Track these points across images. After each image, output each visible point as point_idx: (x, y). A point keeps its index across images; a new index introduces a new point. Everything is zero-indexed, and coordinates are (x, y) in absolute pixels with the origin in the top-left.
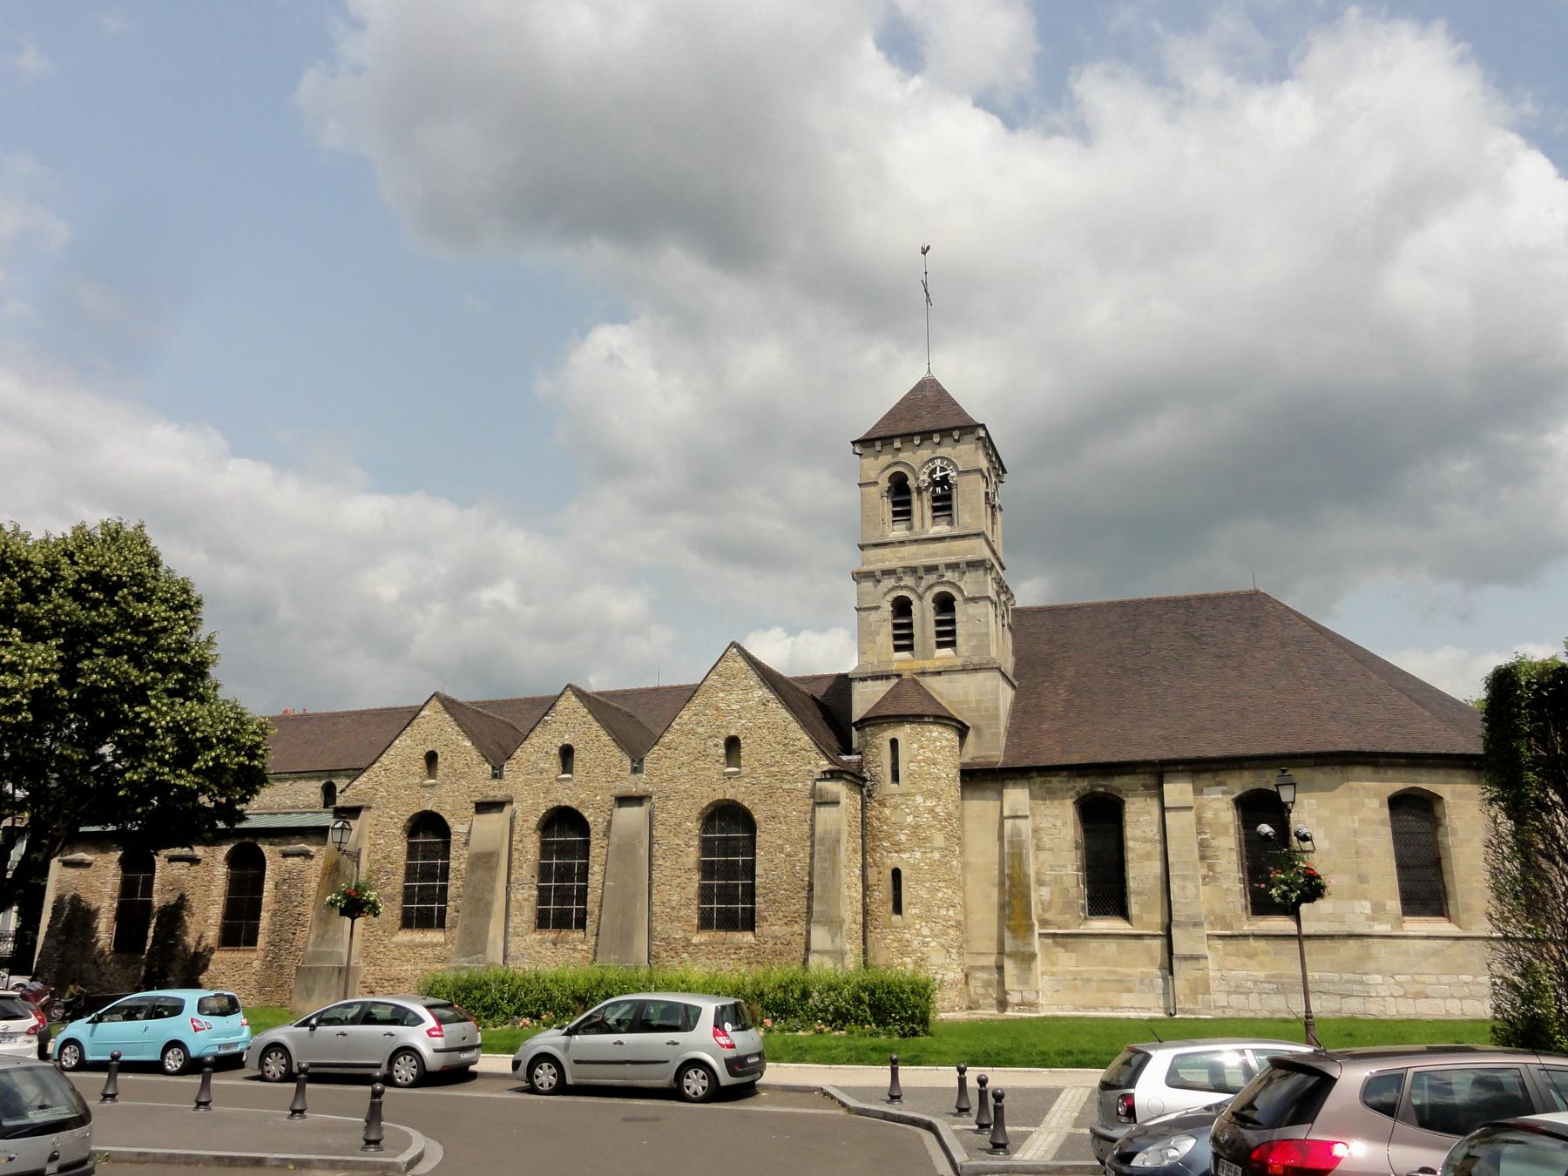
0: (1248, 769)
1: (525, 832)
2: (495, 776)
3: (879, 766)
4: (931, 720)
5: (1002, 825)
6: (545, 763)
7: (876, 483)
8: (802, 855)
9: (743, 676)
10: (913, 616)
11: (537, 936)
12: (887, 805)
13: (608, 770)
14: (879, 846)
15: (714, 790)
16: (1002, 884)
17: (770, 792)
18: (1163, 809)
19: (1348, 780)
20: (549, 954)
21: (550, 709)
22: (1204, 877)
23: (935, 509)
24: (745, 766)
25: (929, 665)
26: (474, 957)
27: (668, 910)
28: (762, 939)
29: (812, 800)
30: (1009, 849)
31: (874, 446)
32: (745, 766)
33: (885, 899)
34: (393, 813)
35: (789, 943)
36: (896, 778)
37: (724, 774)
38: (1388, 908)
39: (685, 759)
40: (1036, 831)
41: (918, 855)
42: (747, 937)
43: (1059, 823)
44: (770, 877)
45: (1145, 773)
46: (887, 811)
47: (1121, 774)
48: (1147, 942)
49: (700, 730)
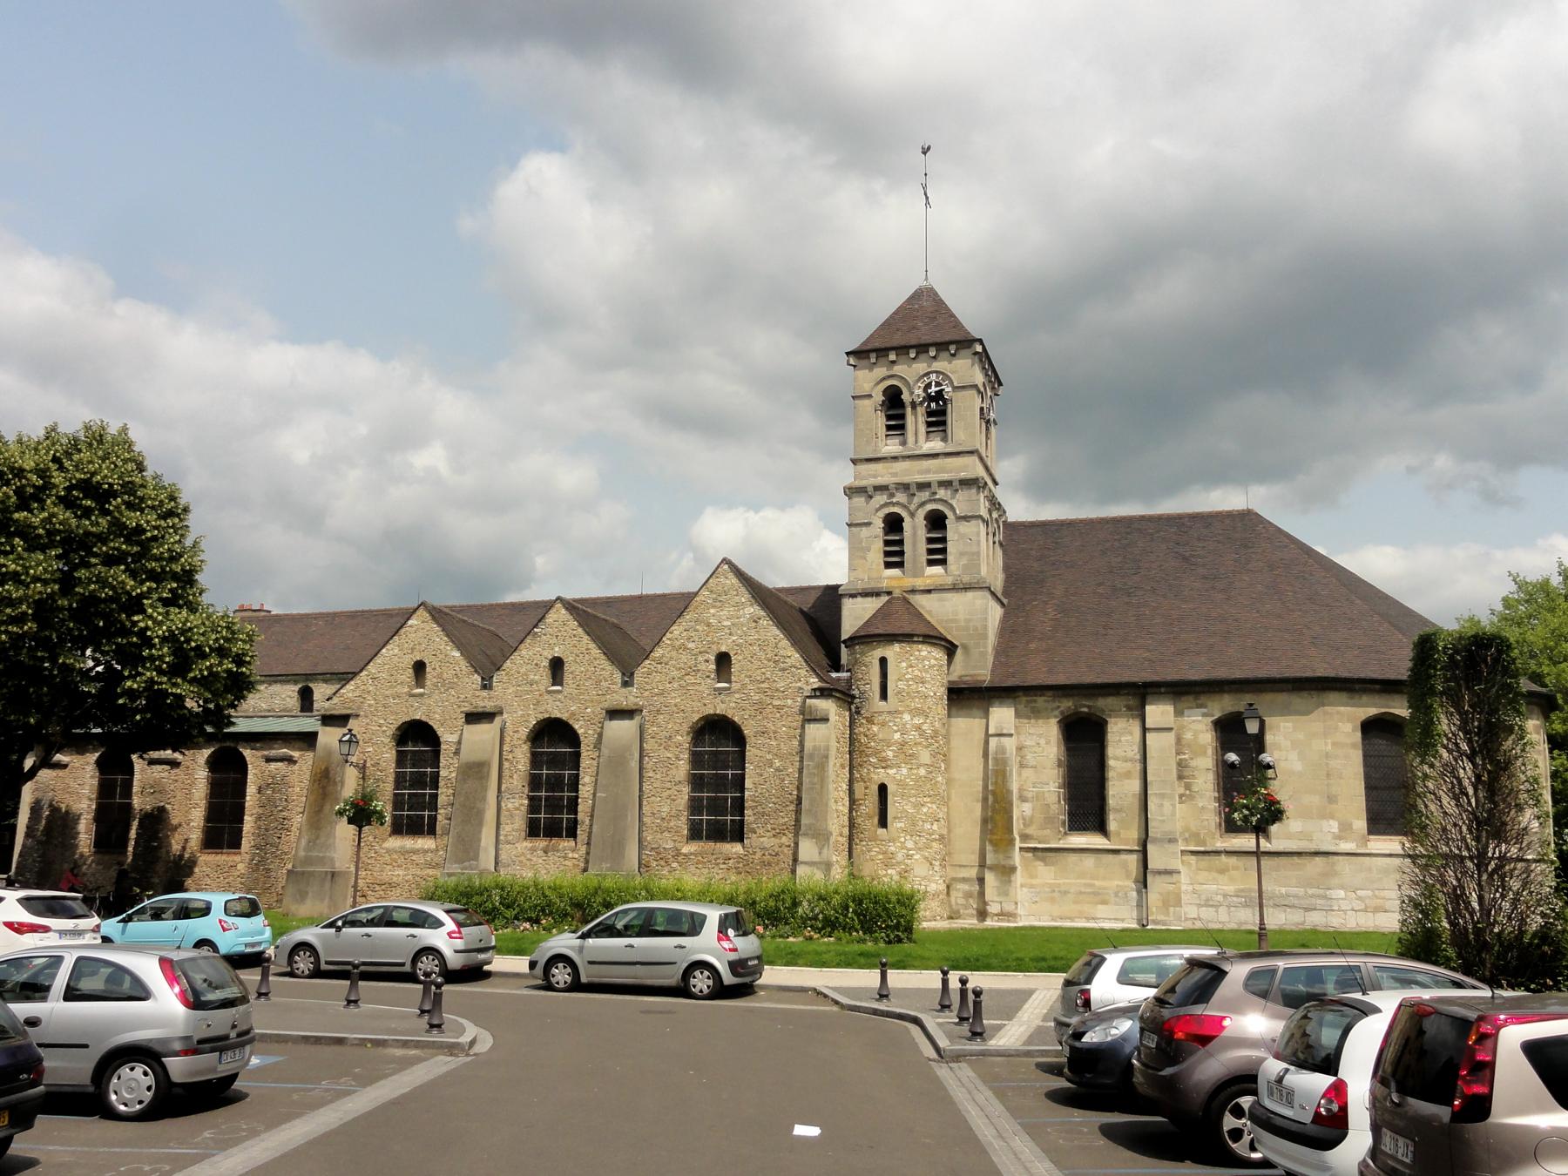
0: (1229, 692)
1: (515, 742)
2: (484, 687)
3: (868, 684)
4: (921, 639)
5: (987, 743)
6: (535, 675)
7: (870, 396)
8: (791, 770)
9: (735, 593)
10: (905, 533)
11: (527, 844)
12: (875, 722)
13: (598, 682)
14: (866, 762)
15: (705, 705)
16: (985, 799)
17: (760, 708)
18: (1144, 730)
19: (1323, 705)
20: (541, 861)
21: (540, 621)
22: (1181, 796)
23: (929, 424)
24: (736, 682)
25: (919, 583)
26: (467, 864)
27: (658, 821)
28: (750, 850)
29: (801, 717)
30: (993, 766)
31: (869, 358)
32: (736, 682)
33: (871, 813)
34: (382, 721)
35: (777, 854)
36: (884, 695)
37: (715, 689)
38: (1354, 827)
40: (1021, 749)
41: (904, 771)
42: (737, 848)
43: (1042, 742)
44: (759, 791)
45: (1128, 694)
46: (875, 728)
48: (1123, 857)
49: (691, 645)
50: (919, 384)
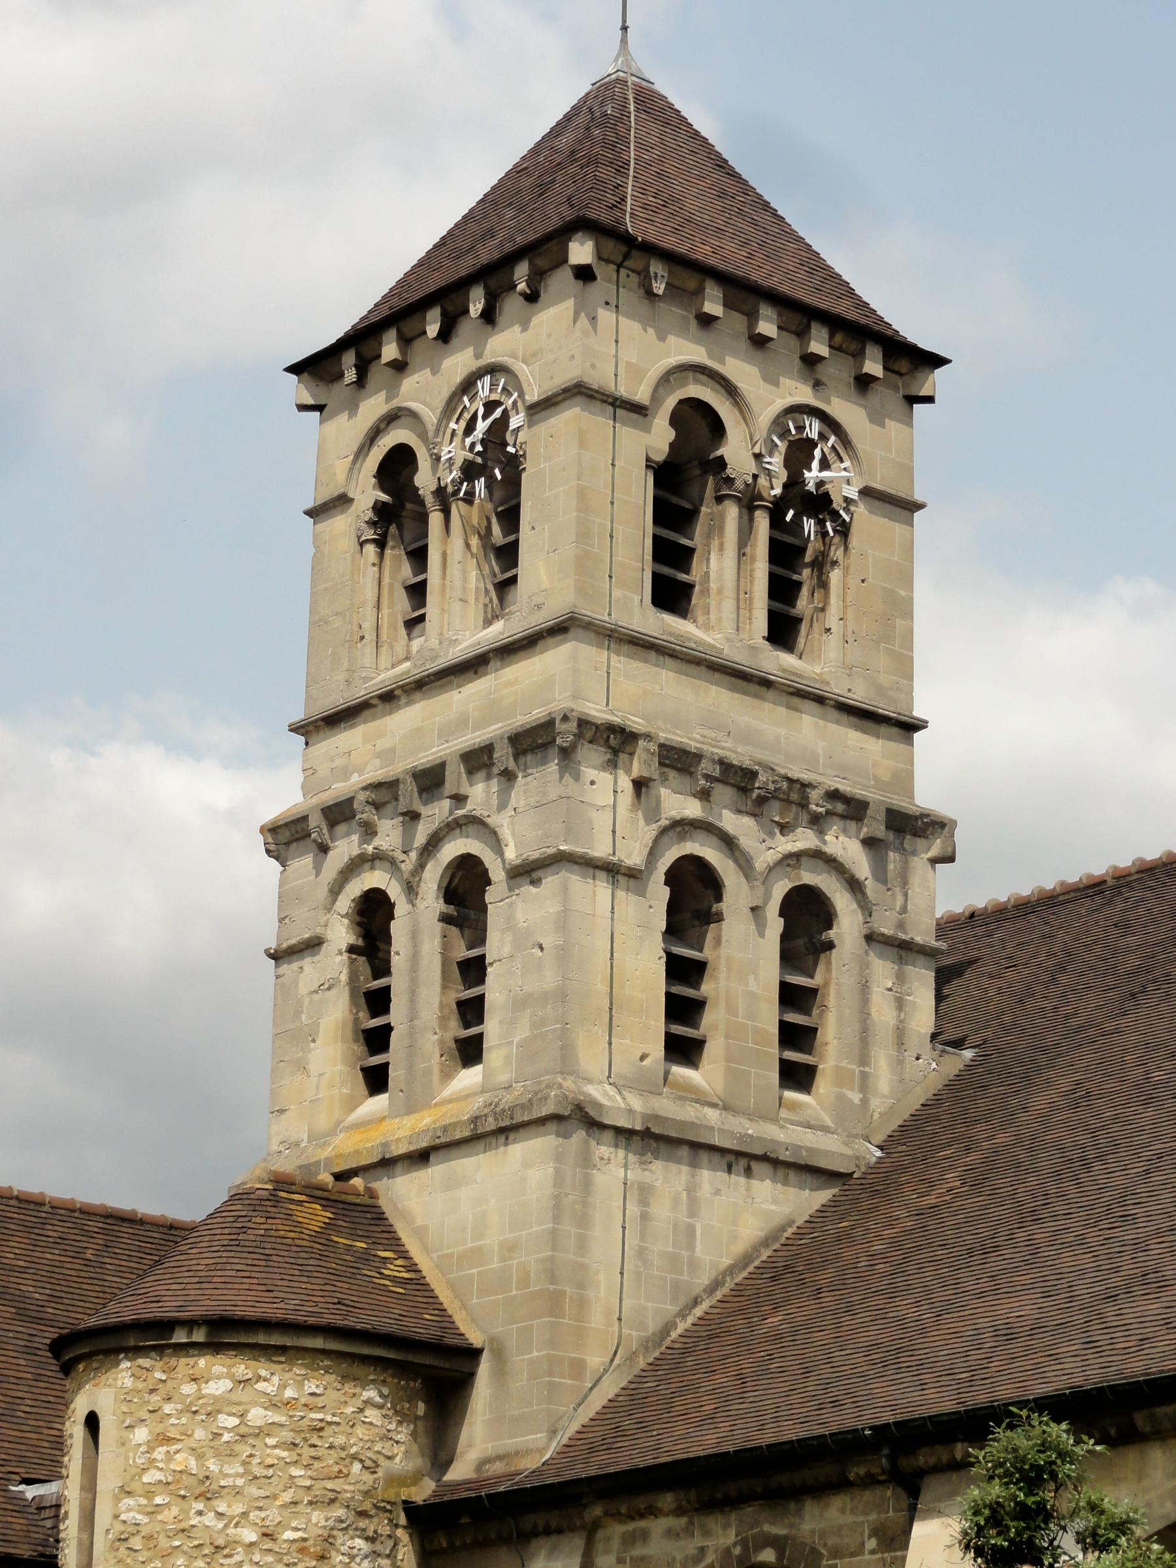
4: (199, 1336)
47: (822, 1490)
50: (453, 425)
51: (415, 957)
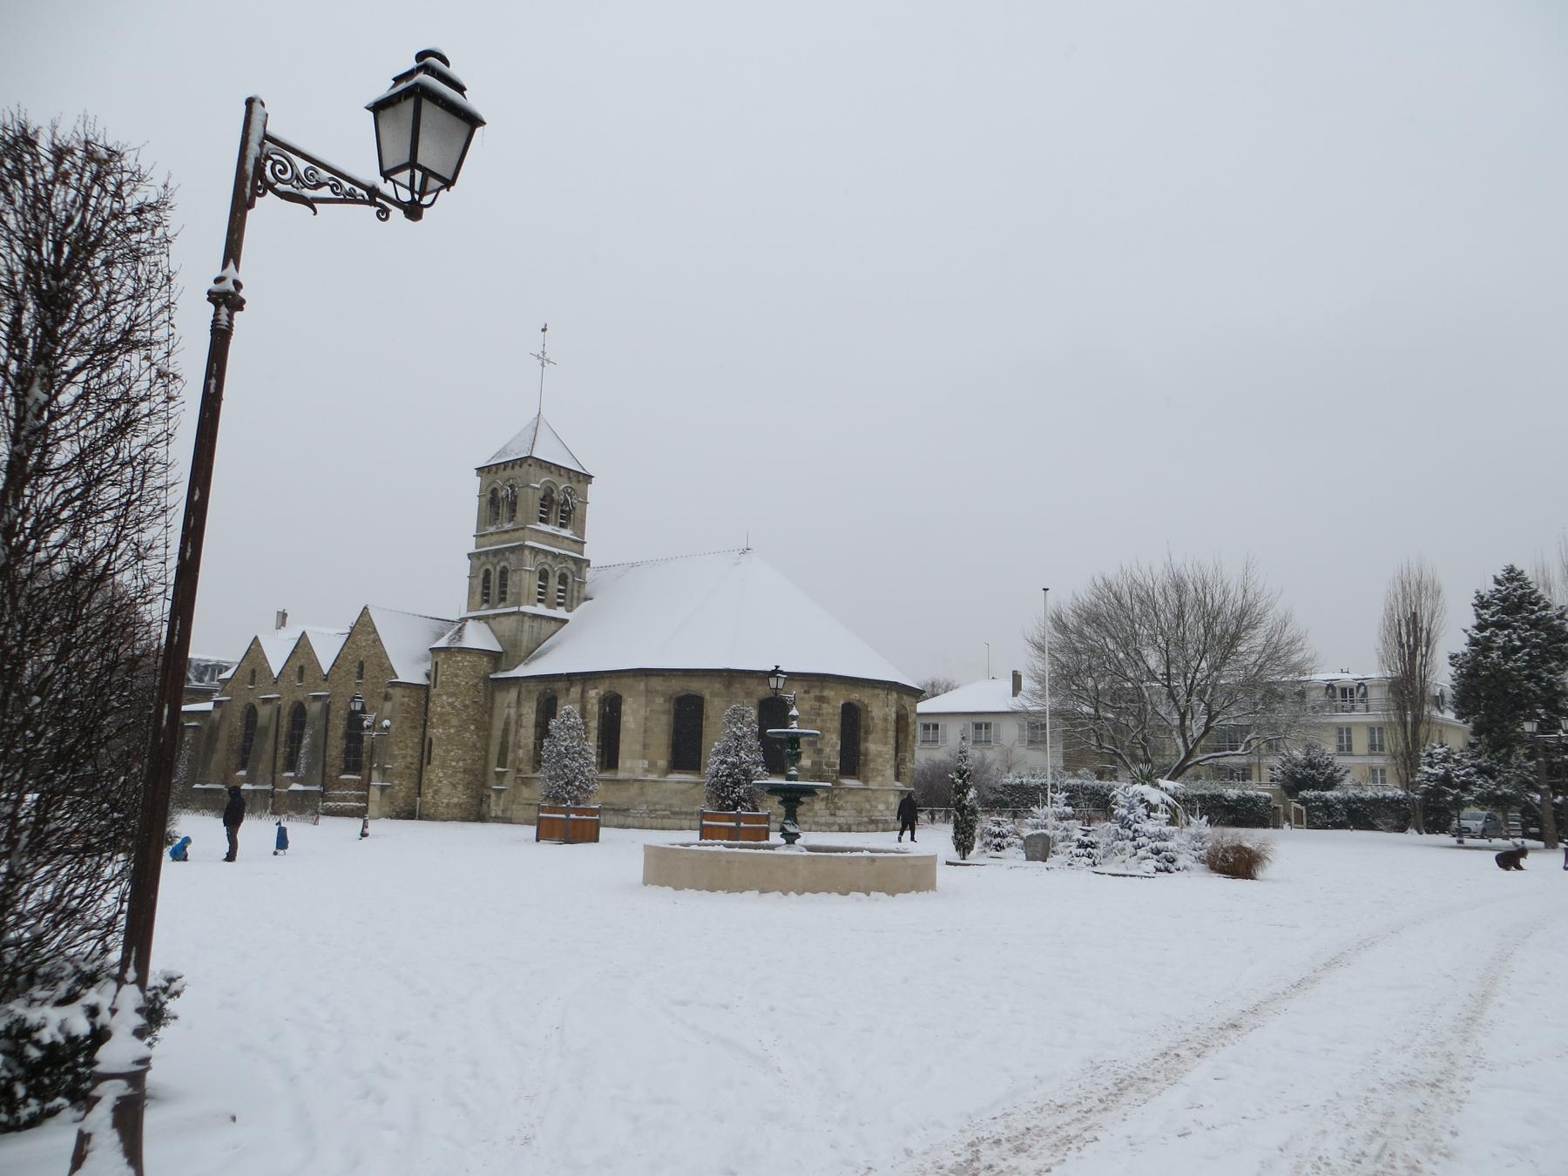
39: (343, 674)
41: (441, 731)
47: (560, 681)
49: (350, 657)
51: (494, 583)
